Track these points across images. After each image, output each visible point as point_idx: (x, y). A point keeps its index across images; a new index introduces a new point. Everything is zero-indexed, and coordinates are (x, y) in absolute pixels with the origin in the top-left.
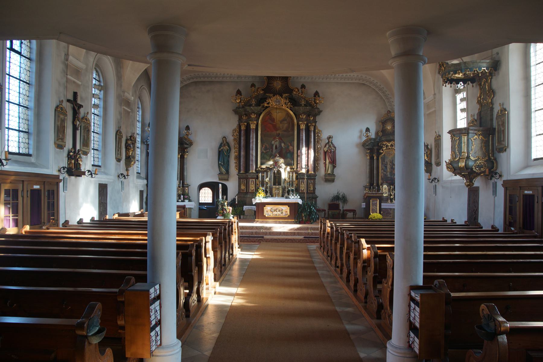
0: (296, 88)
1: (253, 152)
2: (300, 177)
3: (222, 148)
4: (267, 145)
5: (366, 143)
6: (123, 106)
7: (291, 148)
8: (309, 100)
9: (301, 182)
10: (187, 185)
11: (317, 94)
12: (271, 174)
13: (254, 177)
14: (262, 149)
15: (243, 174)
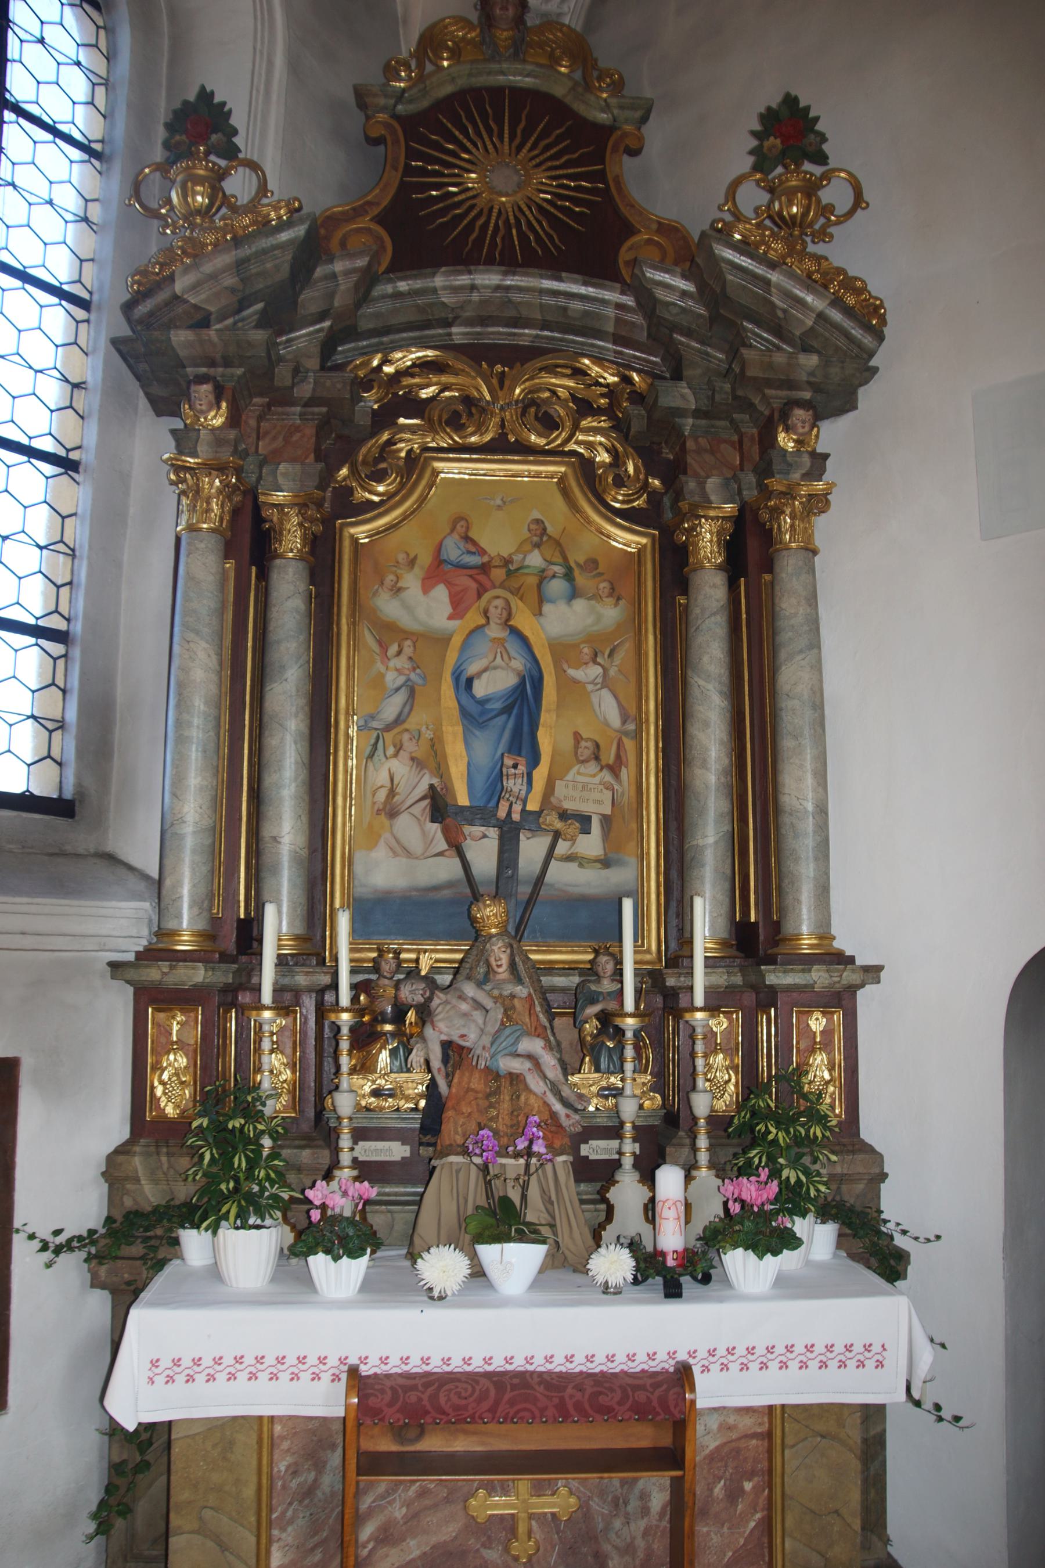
10: (819, 977)
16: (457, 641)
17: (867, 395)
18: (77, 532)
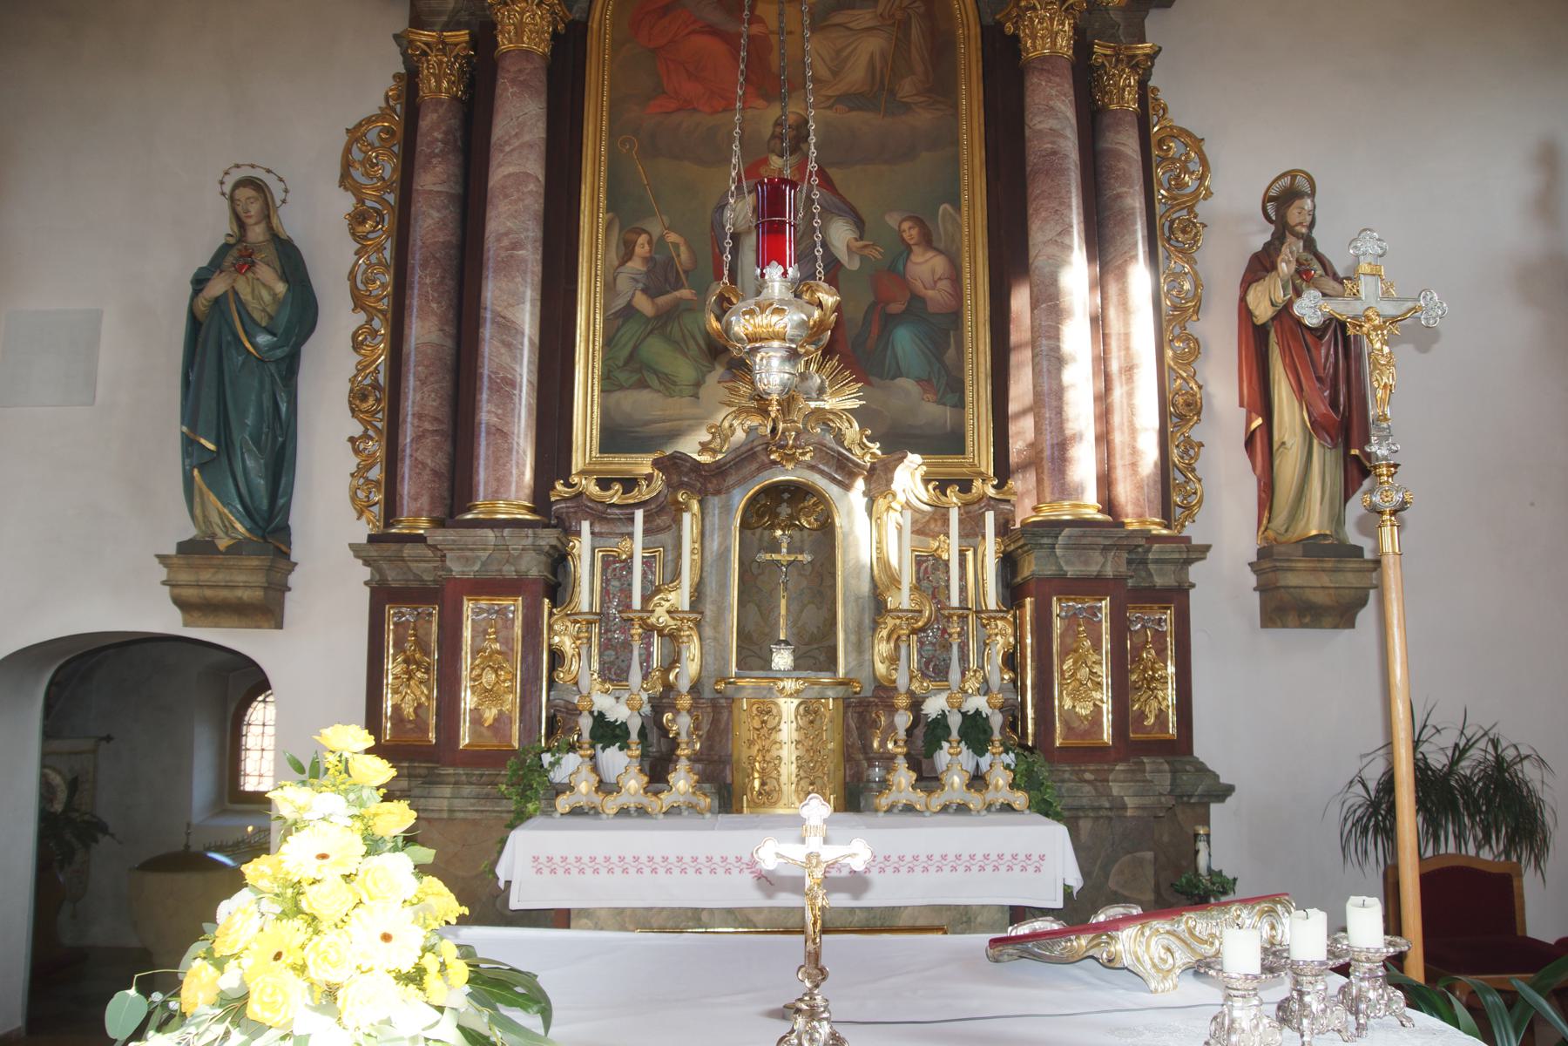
2: (1049, 570)
3: (217, 287)
9: (1071, 619)
12: (714, 545)
13: (509, 571)
14: (623, 283)
15: (409, 550)
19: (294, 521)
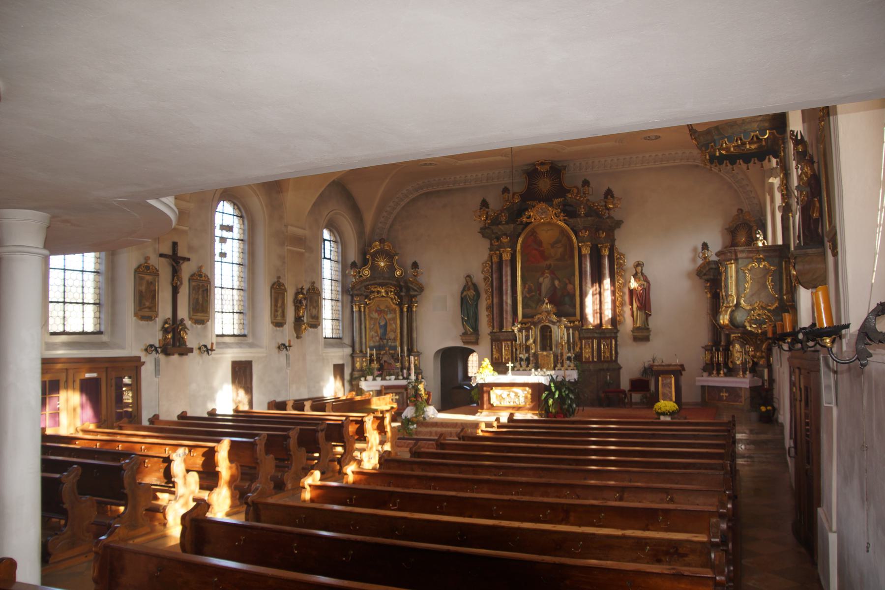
0: (574, 187)
1: (507, 299)
3: (465, 293)
4: (531, 285)
5: (702, 270)
6: (287, 246)
7: (570, 287)
8: (594, 206)
10: (417, 354)
11: (609, 193)
15: (497, 334)
16: (378, 319)
17: (423, 293)
18: (340, 308)
19: (479, 328)
